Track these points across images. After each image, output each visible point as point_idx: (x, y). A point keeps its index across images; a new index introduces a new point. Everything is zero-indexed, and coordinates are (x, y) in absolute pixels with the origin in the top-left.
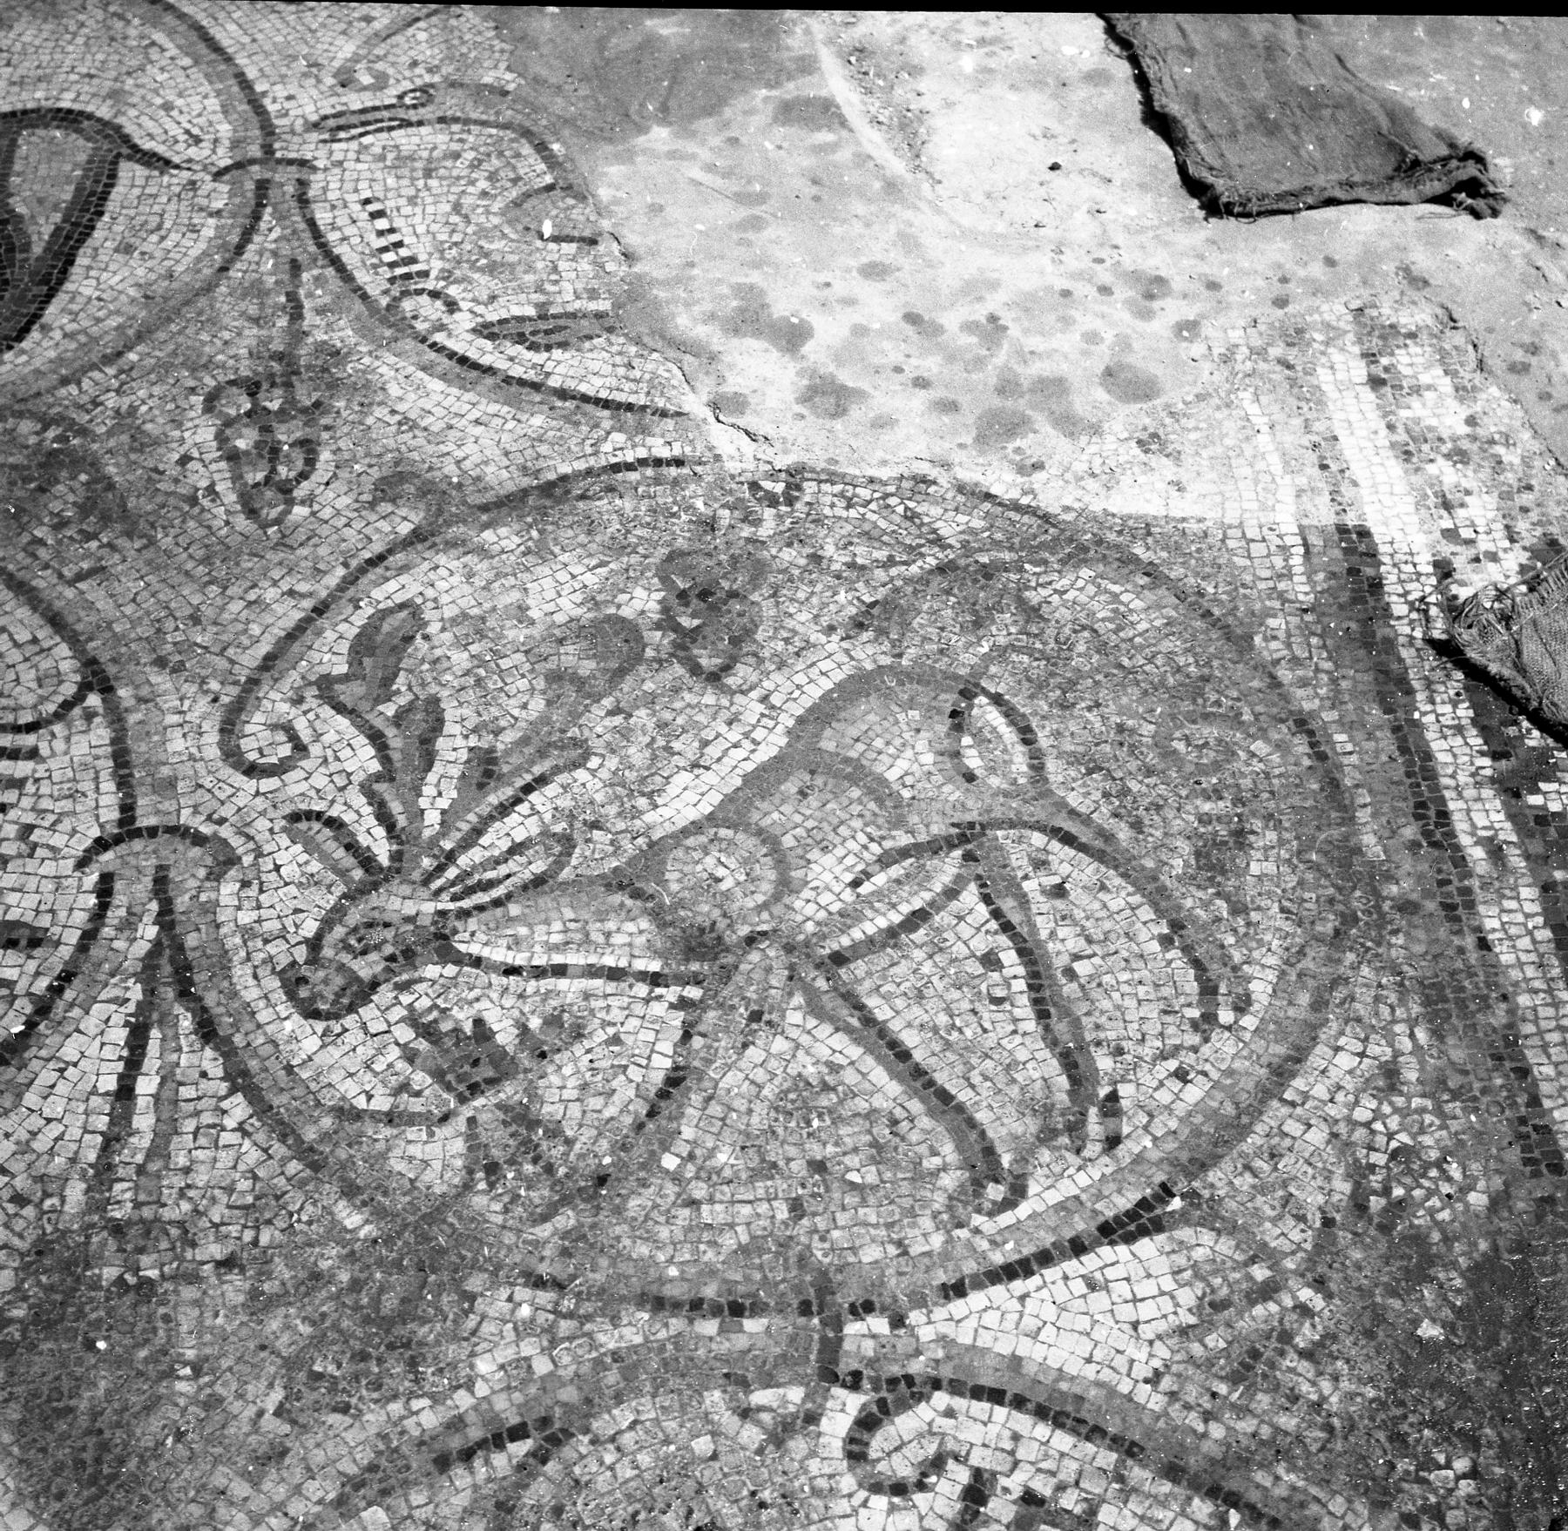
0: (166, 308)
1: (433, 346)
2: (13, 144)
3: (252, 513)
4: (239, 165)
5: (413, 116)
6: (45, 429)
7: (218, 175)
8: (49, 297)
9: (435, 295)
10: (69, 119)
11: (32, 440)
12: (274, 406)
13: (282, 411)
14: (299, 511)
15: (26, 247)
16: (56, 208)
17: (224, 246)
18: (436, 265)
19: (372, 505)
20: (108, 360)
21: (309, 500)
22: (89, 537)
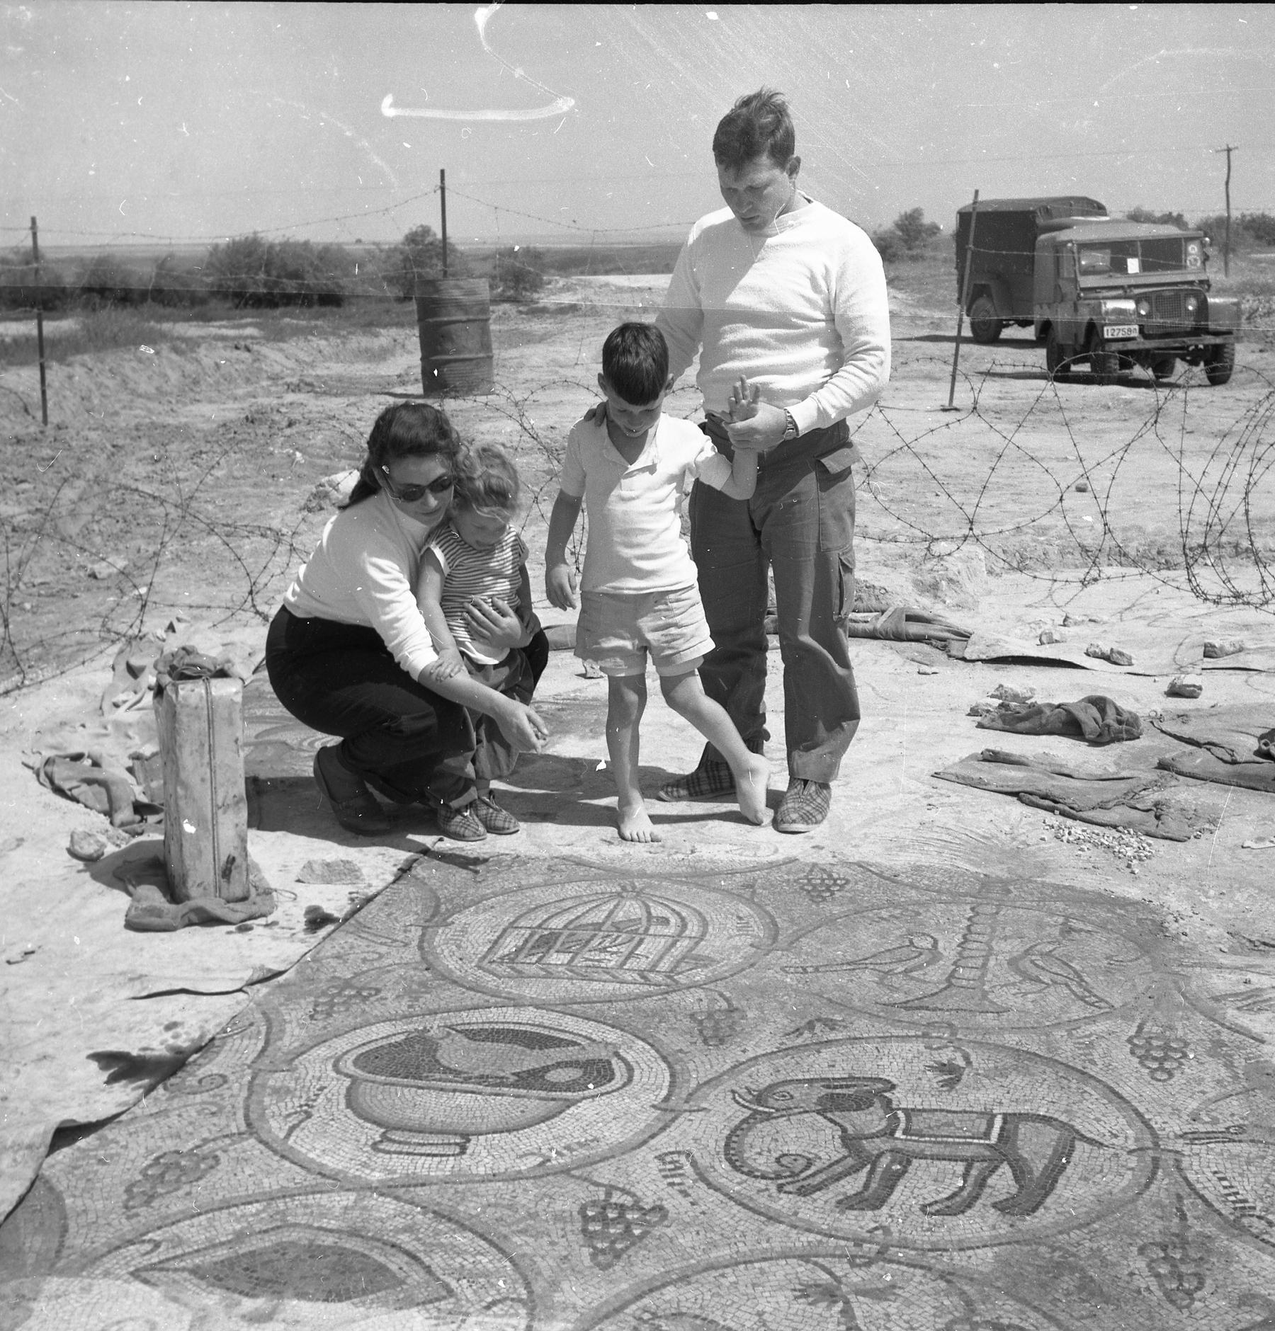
0: (1106, 1208)
1: (1263, 1240)
2: (1017, 1127)
3: (1172, 1302)
4: (1141, 1149)
5: (1235, 1137)
6: (1054, 1251)
7: (1130, 1152)
8: (1047, 1195)
9: (1260, 1218)
10: (1046, 1120)
11: (1047, 1256)
12: (1178, 1256)
13: (1181, 1259)
14: (1198, 1304)
15: (1031, 1172)
16: (1044, 1157)
17: (1139, 1184)
18: (1259, 1205)
19: (1239, 1306)
20: (1080, 1227)
21: (1202, 1300)
22: (1084, 1301)
